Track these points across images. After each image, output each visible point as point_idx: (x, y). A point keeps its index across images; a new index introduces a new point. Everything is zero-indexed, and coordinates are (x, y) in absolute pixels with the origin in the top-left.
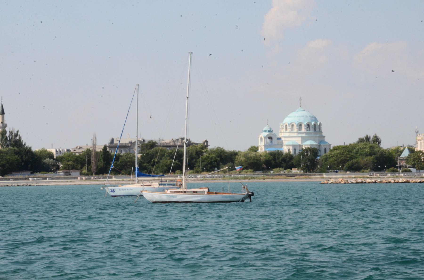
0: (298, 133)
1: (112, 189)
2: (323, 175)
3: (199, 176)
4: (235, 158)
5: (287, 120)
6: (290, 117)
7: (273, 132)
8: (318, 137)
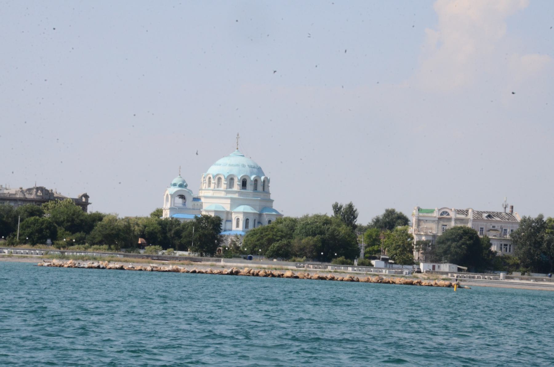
0: (227, 192)
5: (213, 170)
7: (188, 188)
8: (260, 200)
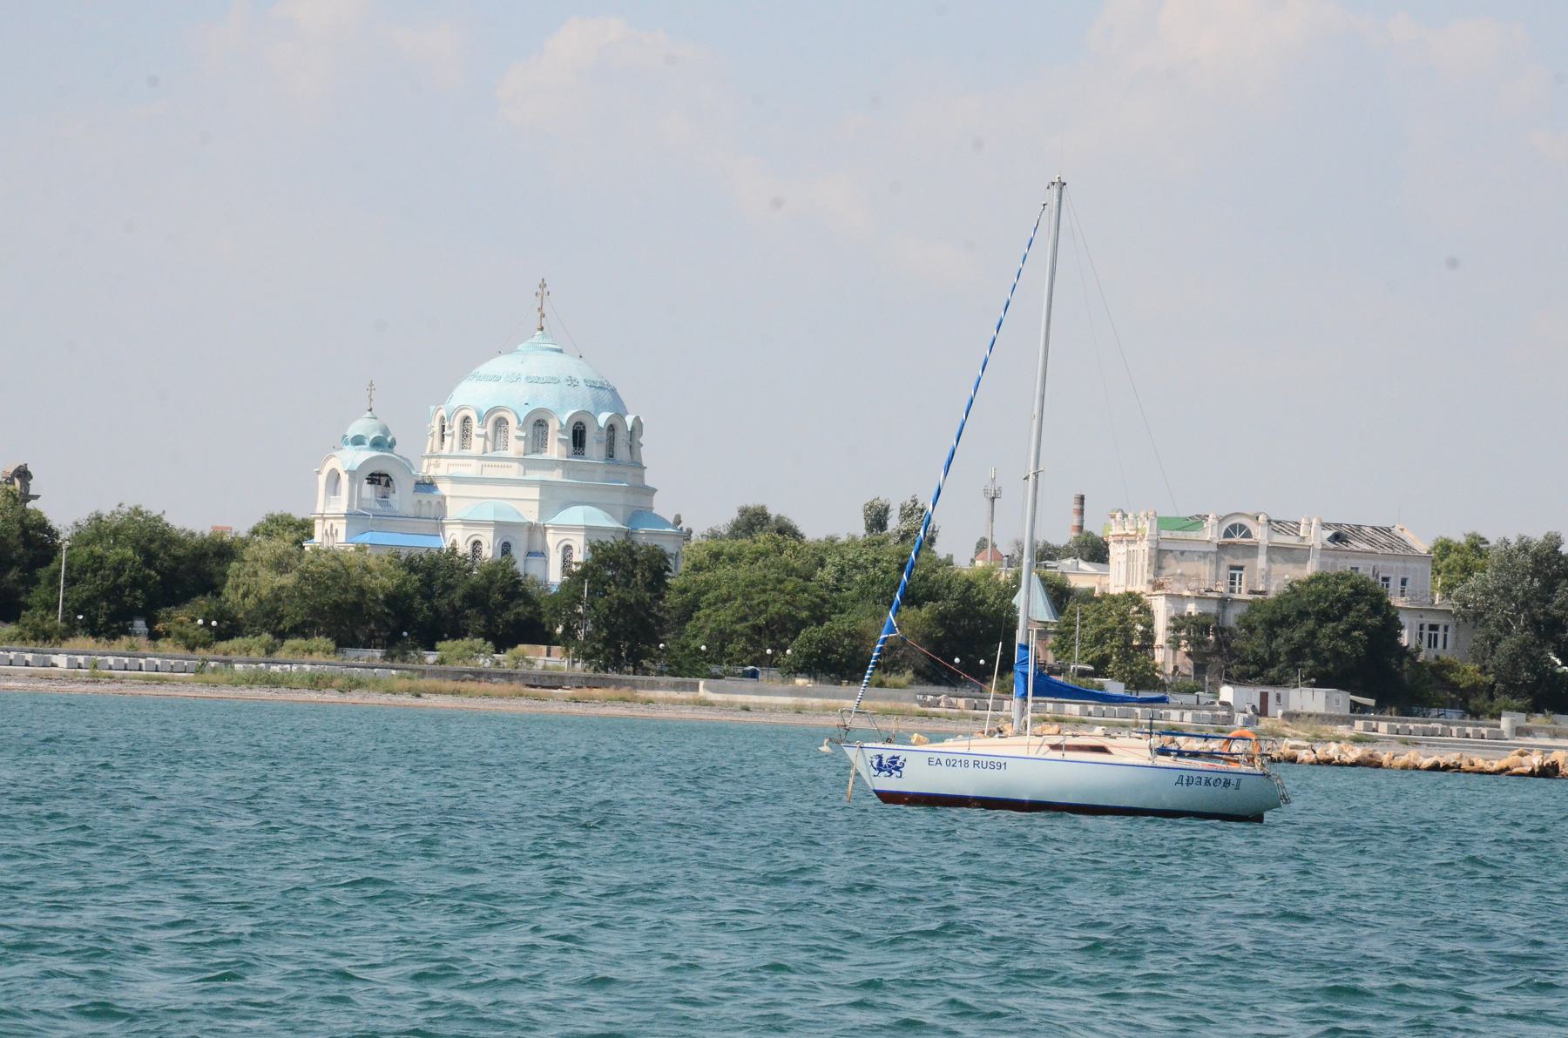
0: (528, 465)
1: (887, 755)
2: (695, 687)
3: (61, 660)
4: (225, 575)
5: (472, 395)
8: (627, 490)
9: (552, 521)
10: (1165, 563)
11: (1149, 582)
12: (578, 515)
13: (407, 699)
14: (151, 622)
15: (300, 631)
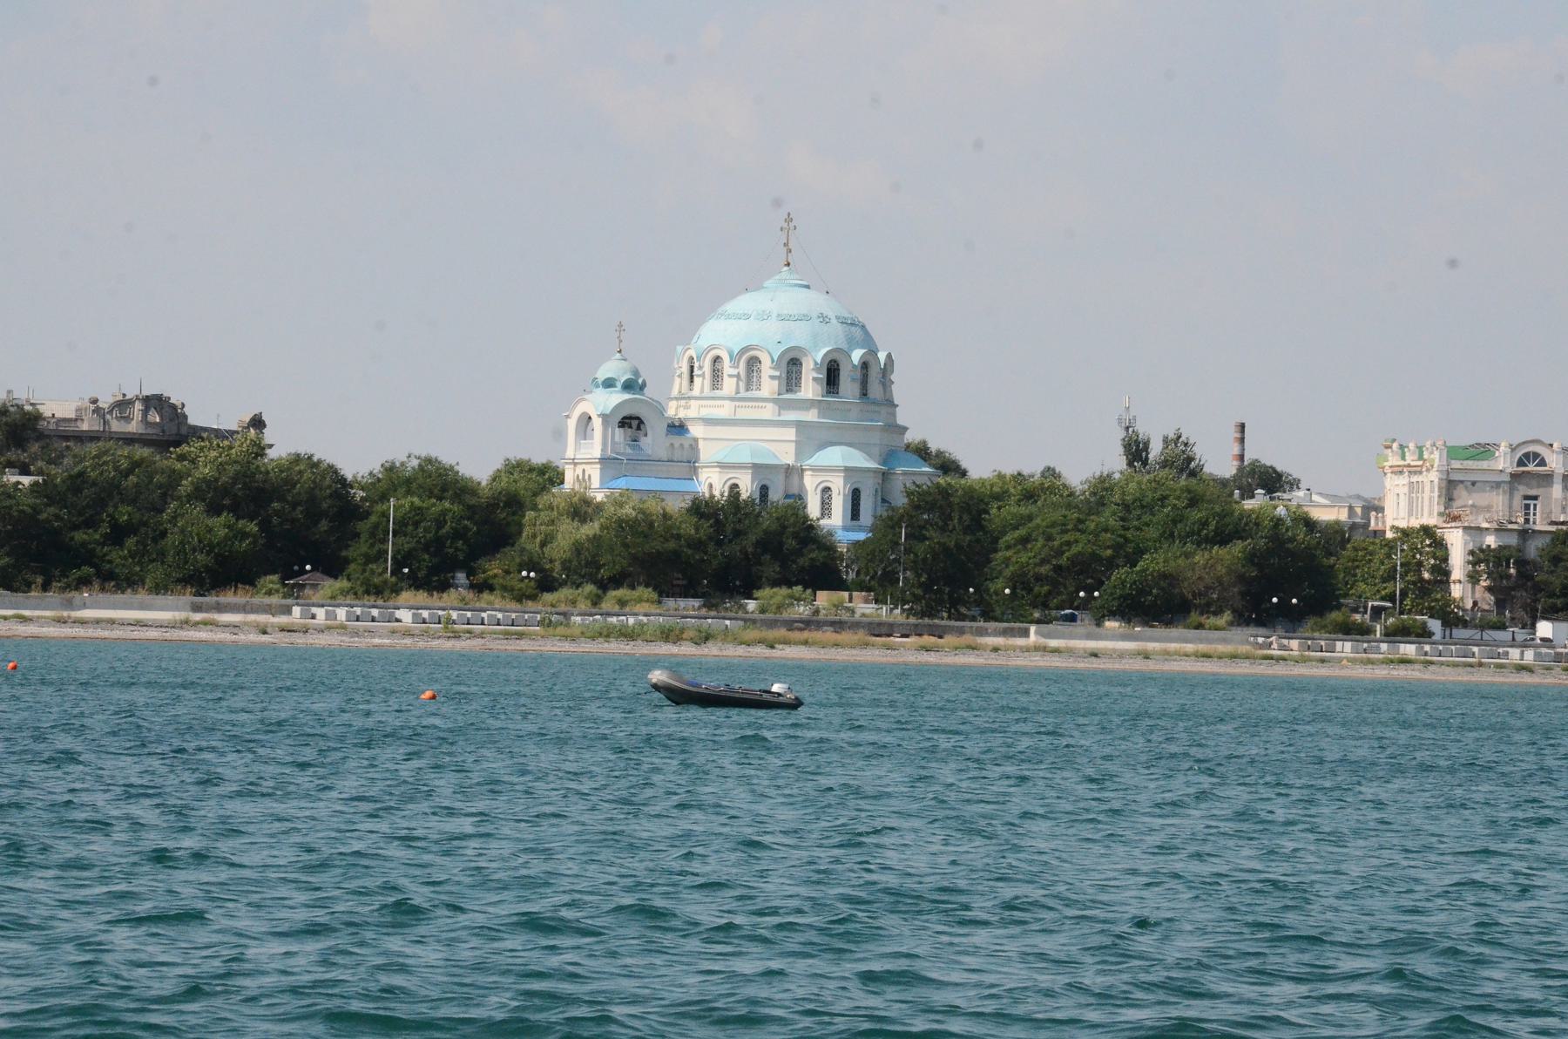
0: (783, 405)
4: (520, 526)
5: (722, 333)
6: (729, 317)
9: (809, 462)
10: (1455, 494)
11: (1440, 514)
12: (836, 456)
13: (760, 651)
14: (471, 573)
15: (617, 581)
